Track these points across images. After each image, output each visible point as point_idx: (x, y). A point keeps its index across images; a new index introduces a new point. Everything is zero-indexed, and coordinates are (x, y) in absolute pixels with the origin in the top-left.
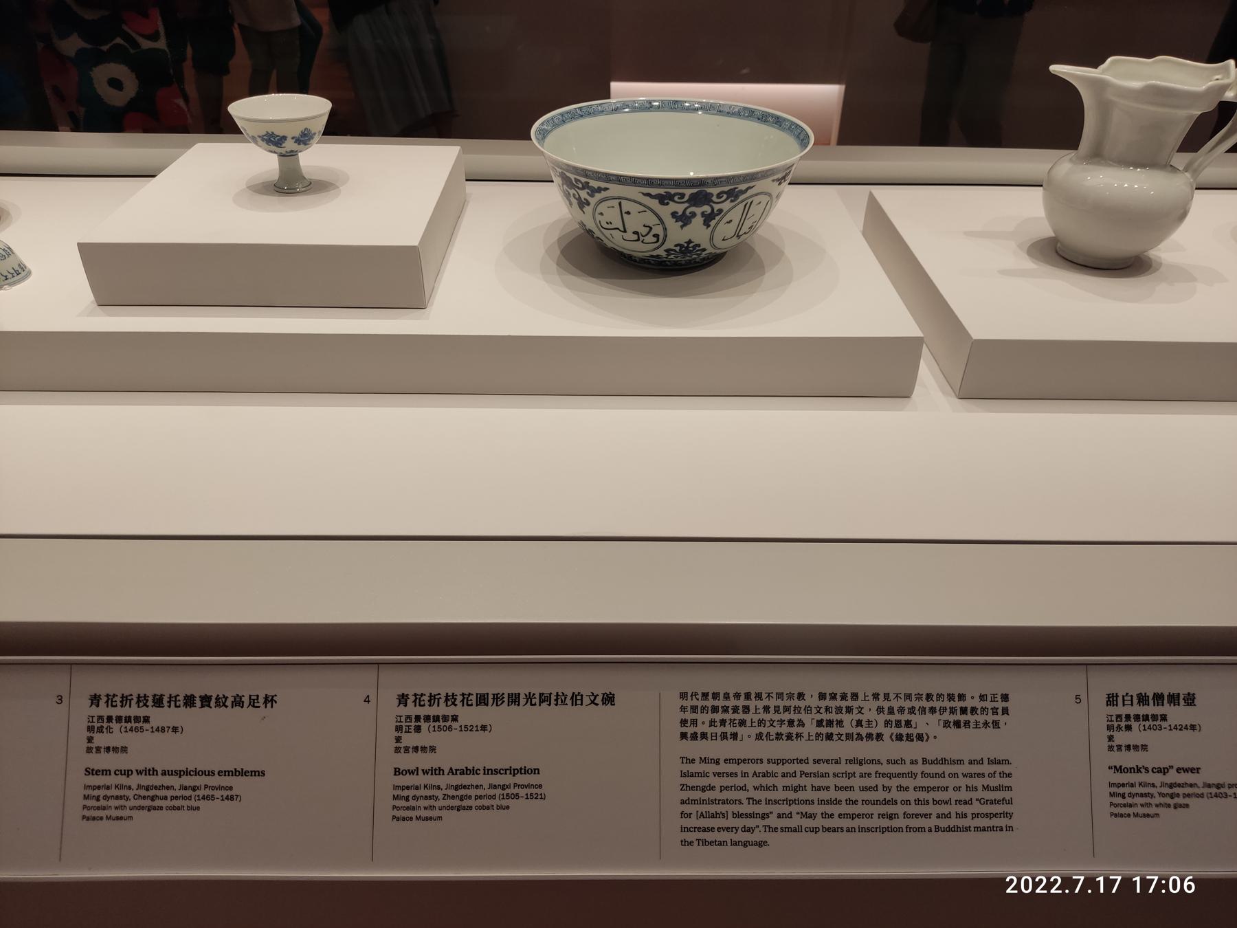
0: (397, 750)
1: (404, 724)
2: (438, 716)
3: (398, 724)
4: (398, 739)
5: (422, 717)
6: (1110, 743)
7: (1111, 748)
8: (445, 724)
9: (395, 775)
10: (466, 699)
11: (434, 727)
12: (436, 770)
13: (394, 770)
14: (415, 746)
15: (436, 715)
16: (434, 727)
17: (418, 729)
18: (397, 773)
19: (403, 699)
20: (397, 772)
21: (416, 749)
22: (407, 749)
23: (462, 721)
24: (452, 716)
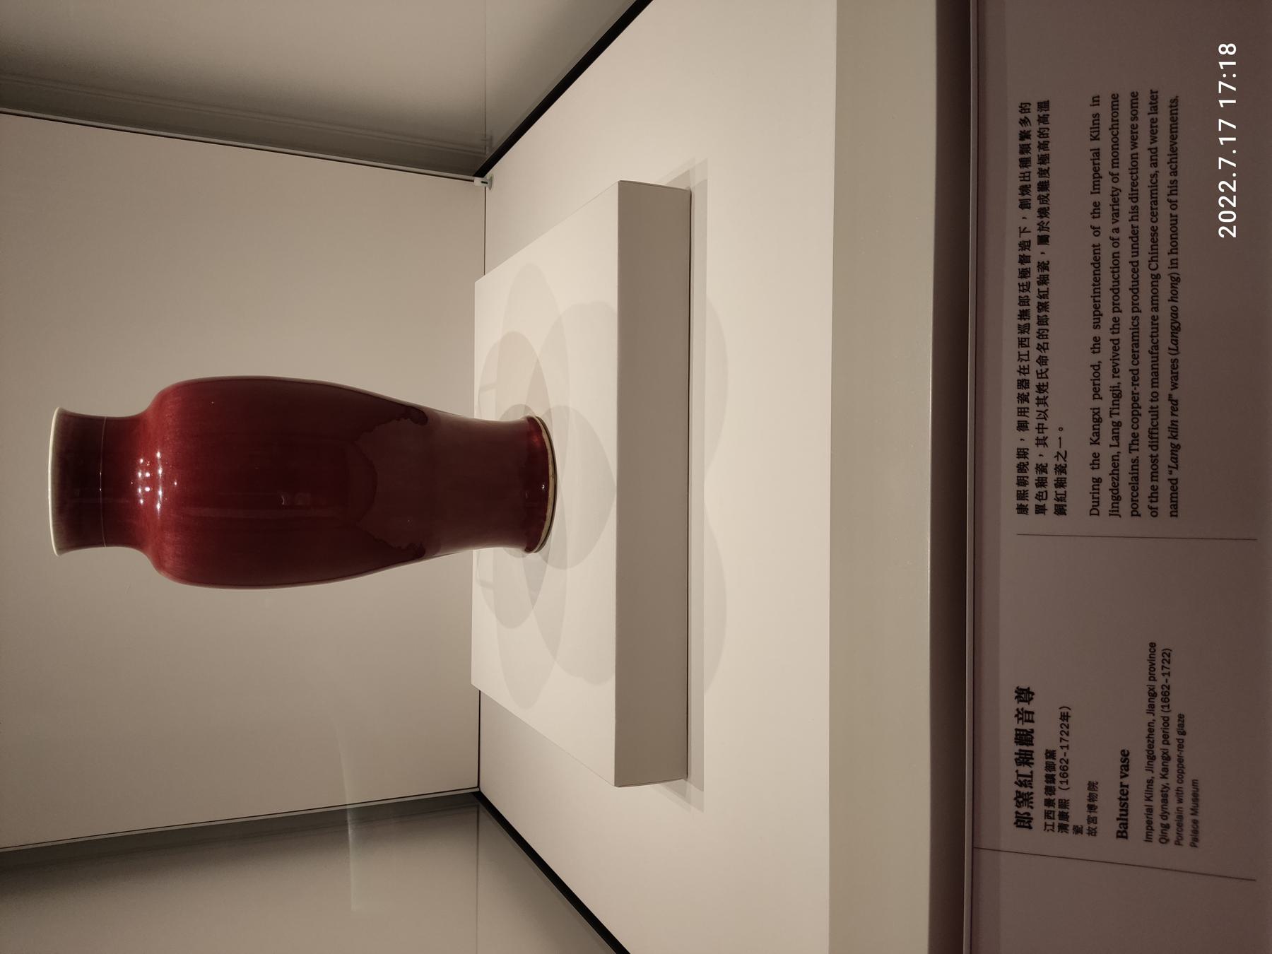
0: (1092, 832)
1: (1057, 821)
2: (1047, 776)
3: (1056, 828)
4: (1078, 830)
8: (1057, 767)
9: (1126, 837)
11: (1061, 782)
13: (1119, 839)
16: (1061, 782)
18: (1124, 834)
19: (1023, 821)
20: (1122, 834)
21: (1091, 808)
22: (1092, 820)
23: (1054, 745)
24: (1047, 758)
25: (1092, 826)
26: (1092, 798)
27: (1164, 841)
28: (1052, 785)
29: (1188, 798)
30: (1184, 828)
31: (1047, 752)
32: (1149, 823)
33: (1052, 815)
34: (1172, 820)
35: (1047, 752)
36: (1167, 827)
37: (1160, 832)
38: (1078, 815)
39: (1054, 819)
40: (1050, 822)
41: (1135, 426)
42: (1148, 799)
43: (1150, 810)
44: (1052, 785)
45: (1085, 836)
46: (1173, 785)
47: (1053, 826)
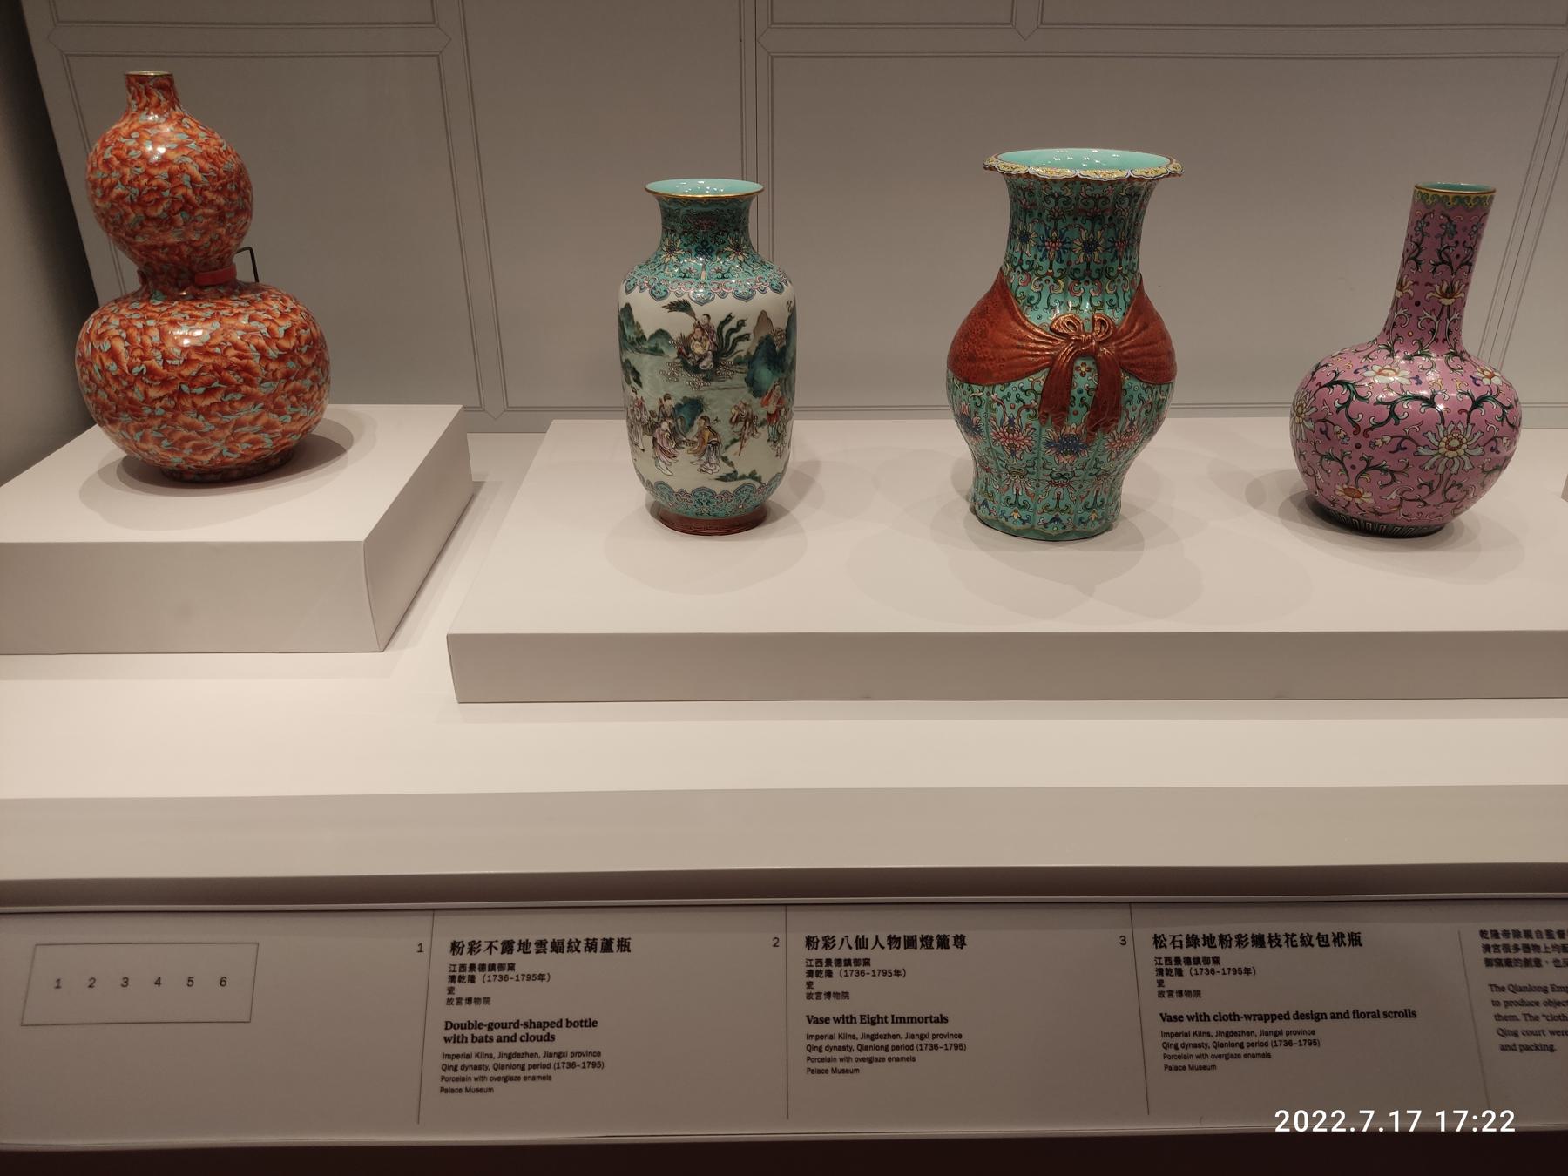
0: (449, 1002)
1: (457, 974)
2: (494, 965)
3: (452, 974)
4: (451, 990)
6: (1161, 989)
7: (1161, 994)
8: (501, 973)
10: (524, 946)
13: (444, 1024)
14: (468, 997)
16: (489, 976)
17: (472, 979)
19: (455, 947)
21: (469, 1000)
23: (519, 970)
24: (509, 964)
26: (477, 1000)
31: (513, 965)
35: (513, 965)
38: (463, 990)
39: (460, 971)
40: (457, 968)
47: (454, 971)
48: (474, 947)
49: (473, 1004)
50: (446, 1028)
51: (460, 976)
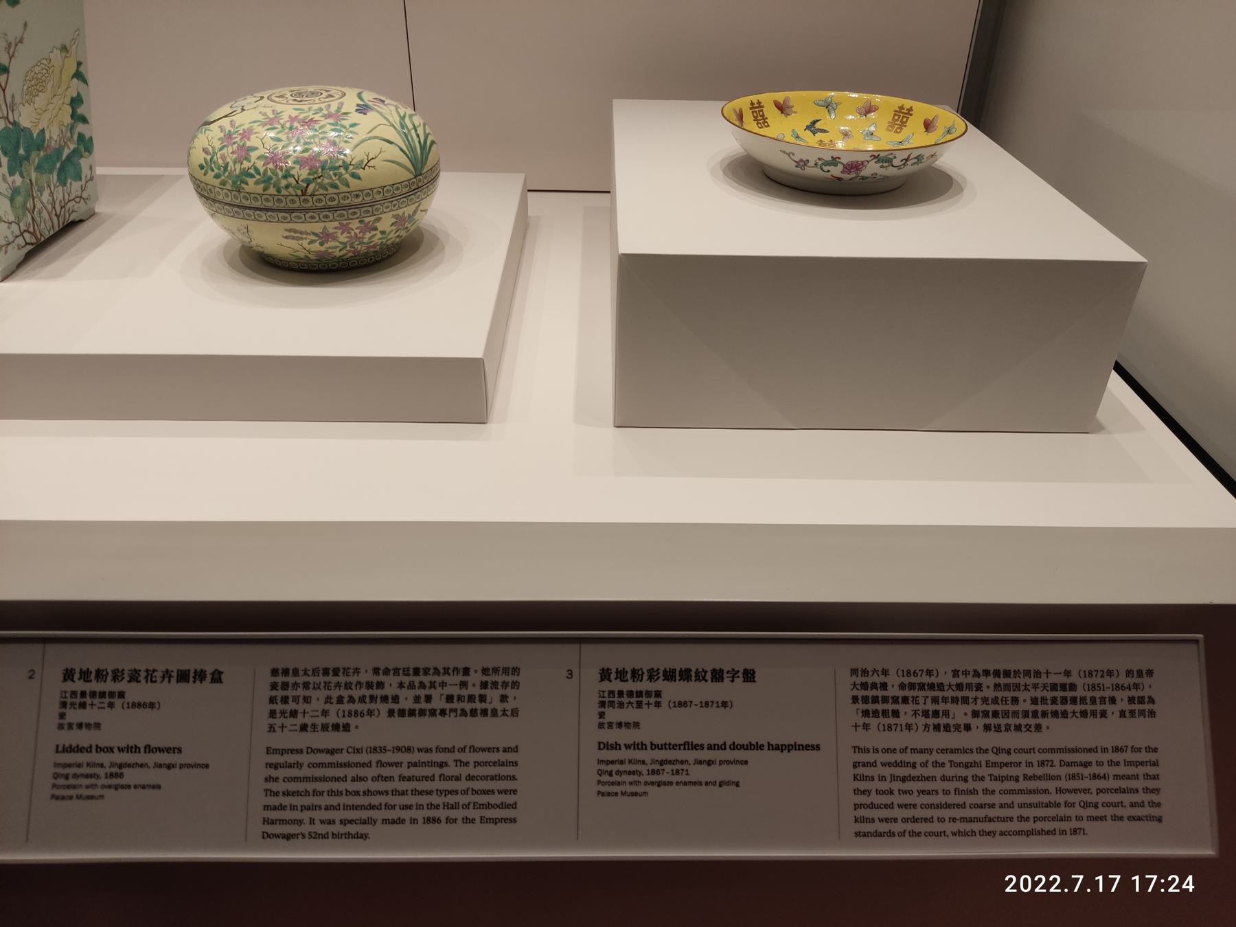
0: (601, 726)
1: (607, 700)
2: (641, 692)
3: (601, 699)
4: (602, 715)
5: (625, 693)
12: (638, 744)
13: (597, 744)
14: (619, 721)
15: (639, 690)
19: (605, 675)
21: (620, 725)
22: (610, 725)
24: (655, 692)
25: (606, 726)
27: (600, 772)
28: (635, 696)
29: (634, 789)
30: (611, 787)
32: (612, 762)
33: (611, 696)
34: (615, 778)
36: (611, 775)
37: (605, 770)
38: (613, 715)
40: (606, 694)
41: (1041, 751)
42: (630, 761)
43: (622, 762)
44: (635, 696)
45: (597, 720)
46: (642, 779)
47: (604, 697)
48: (621, 675)
49: (623, 728)
50: (599, 749)
51: (609, 702)
